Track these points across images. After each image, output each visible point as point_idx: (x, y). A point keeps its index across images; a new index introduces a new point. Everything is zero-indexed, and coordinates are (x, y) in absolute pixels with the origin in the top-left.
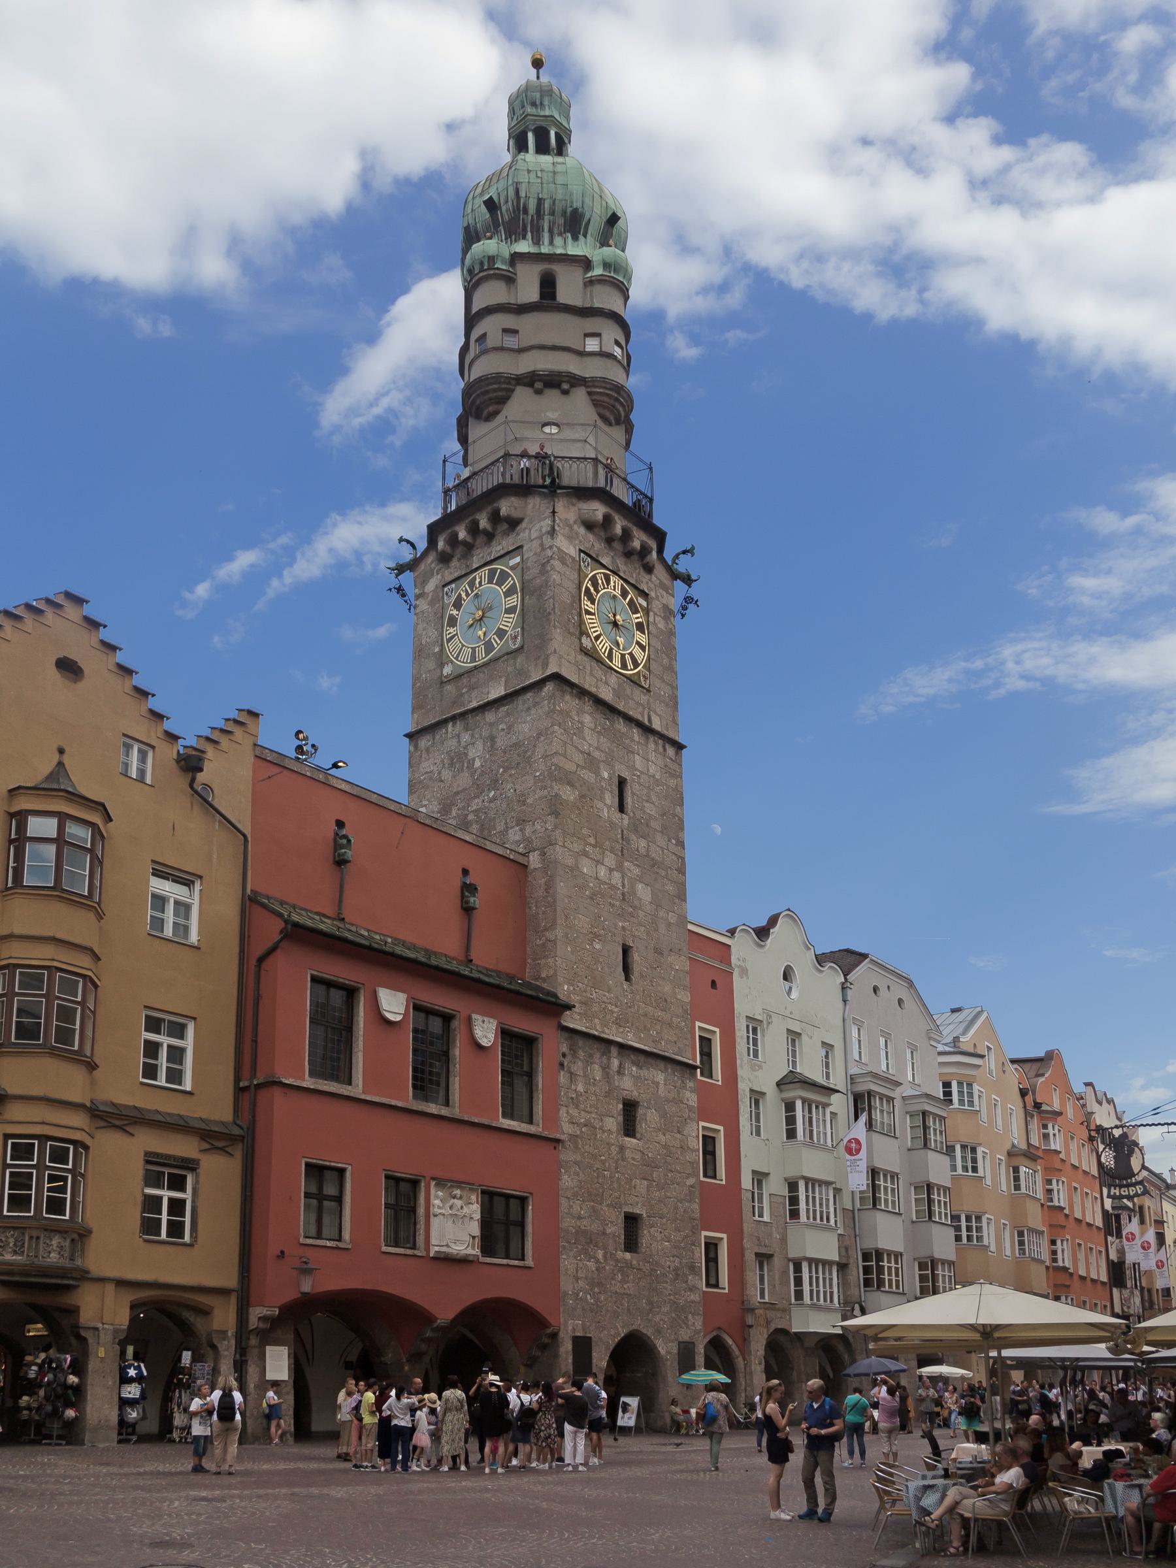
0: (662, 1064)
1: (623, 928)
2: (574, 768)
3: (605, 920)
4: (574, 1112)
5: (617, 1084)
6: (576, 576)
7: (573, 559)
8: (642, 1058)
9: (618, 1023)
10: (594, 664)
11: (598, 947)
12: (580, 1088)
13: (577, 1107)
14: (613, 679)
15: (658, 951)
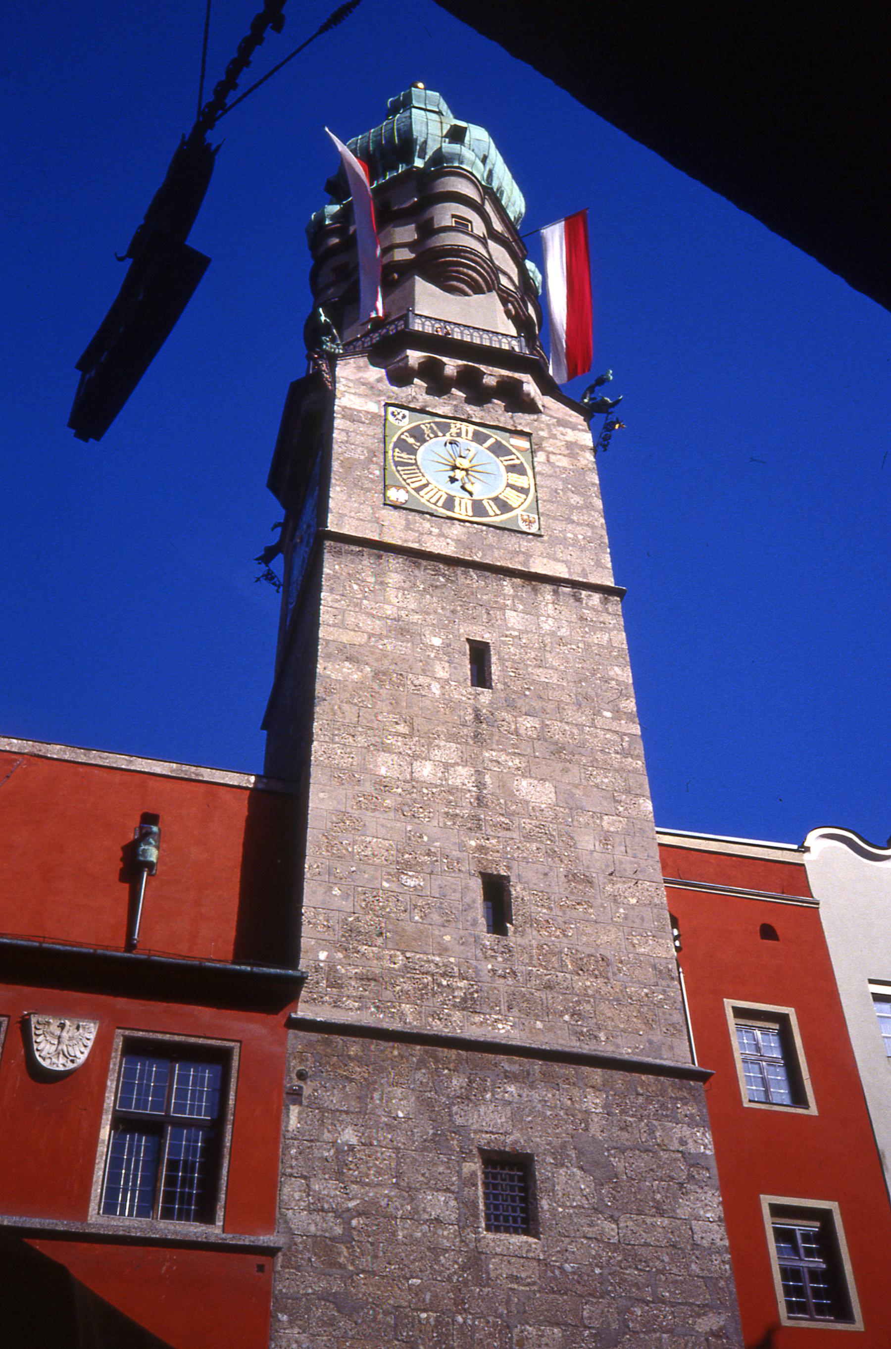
0: (597, 1075)
1: (481, 849)
2: (362, 639)
3: (432, 840)
4: (326, 1187)
5: (459, 1121)
6: (379, 430)
7: (375, 416)
8: (537, 1066)
9: (468, 1005)
10: (411, 516)
11: (412, 883)
12: (349, 1136)
13: (339, 1175)
14: (457, 530)
15: (579, 879)
